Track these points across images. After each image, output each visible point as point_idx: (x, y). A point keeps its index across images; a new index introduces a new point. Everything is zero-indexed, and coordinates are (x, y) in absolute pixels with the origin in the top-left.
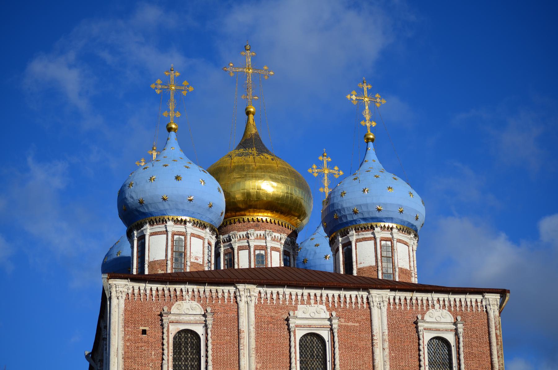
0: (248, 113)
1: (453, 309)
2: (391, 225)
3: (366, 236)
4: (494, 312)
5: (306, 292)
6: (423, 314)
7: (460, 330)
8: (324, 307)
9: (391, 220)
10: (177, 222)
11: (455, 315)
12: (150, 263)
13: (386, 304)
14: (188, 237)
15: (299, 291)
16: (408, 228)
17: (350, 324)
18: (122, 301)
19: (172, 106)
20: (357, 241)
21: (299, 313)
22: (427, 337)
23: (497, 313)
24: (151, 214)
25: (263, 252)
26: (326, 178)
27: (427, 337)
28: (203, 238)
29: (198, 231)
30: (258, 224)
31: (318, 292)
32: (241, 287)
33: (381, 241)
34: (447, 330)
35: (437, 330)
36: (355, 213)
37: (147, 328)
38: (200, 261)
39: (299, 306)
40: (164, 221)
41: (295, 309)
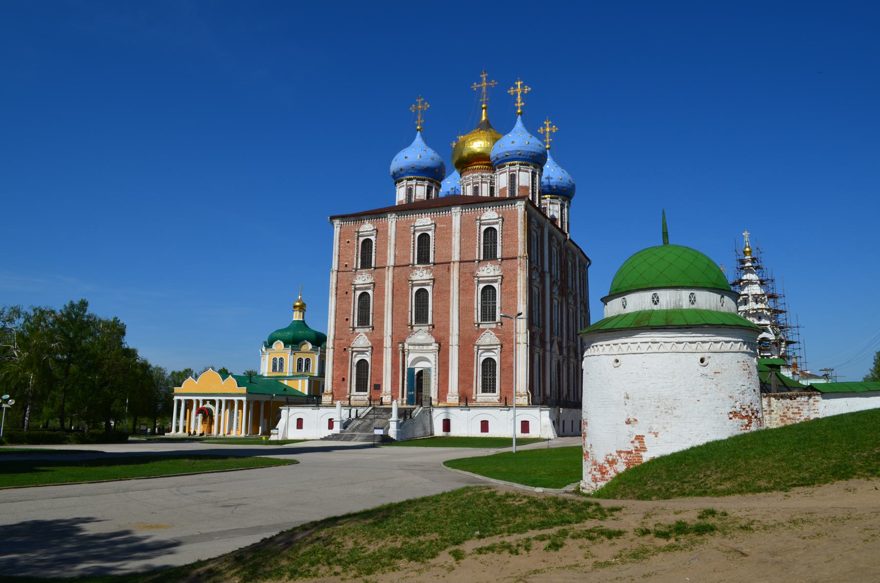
1: (498, 210)
2: (514, 162)
3: (503, 171)
6: (481, 216)
8: (429, 219)
10: (408, 180)
11: (499, 213)
13: (460, 213)
14: (414, 186)
17: (442, 226)
18: (339, 228)
19: (419, 117)
20: (500, 174)
23: (523, 210)
25: (477, 185)
26: (548, 134)
28: (424, 186)
29: (419, 182)
30: (474, 171)
33: (509, 172)
34: (494, 224)
35: (489, 224)
37: (349, 240)
38: (422, 198)
39: (417, 220)
41: (416, 221)
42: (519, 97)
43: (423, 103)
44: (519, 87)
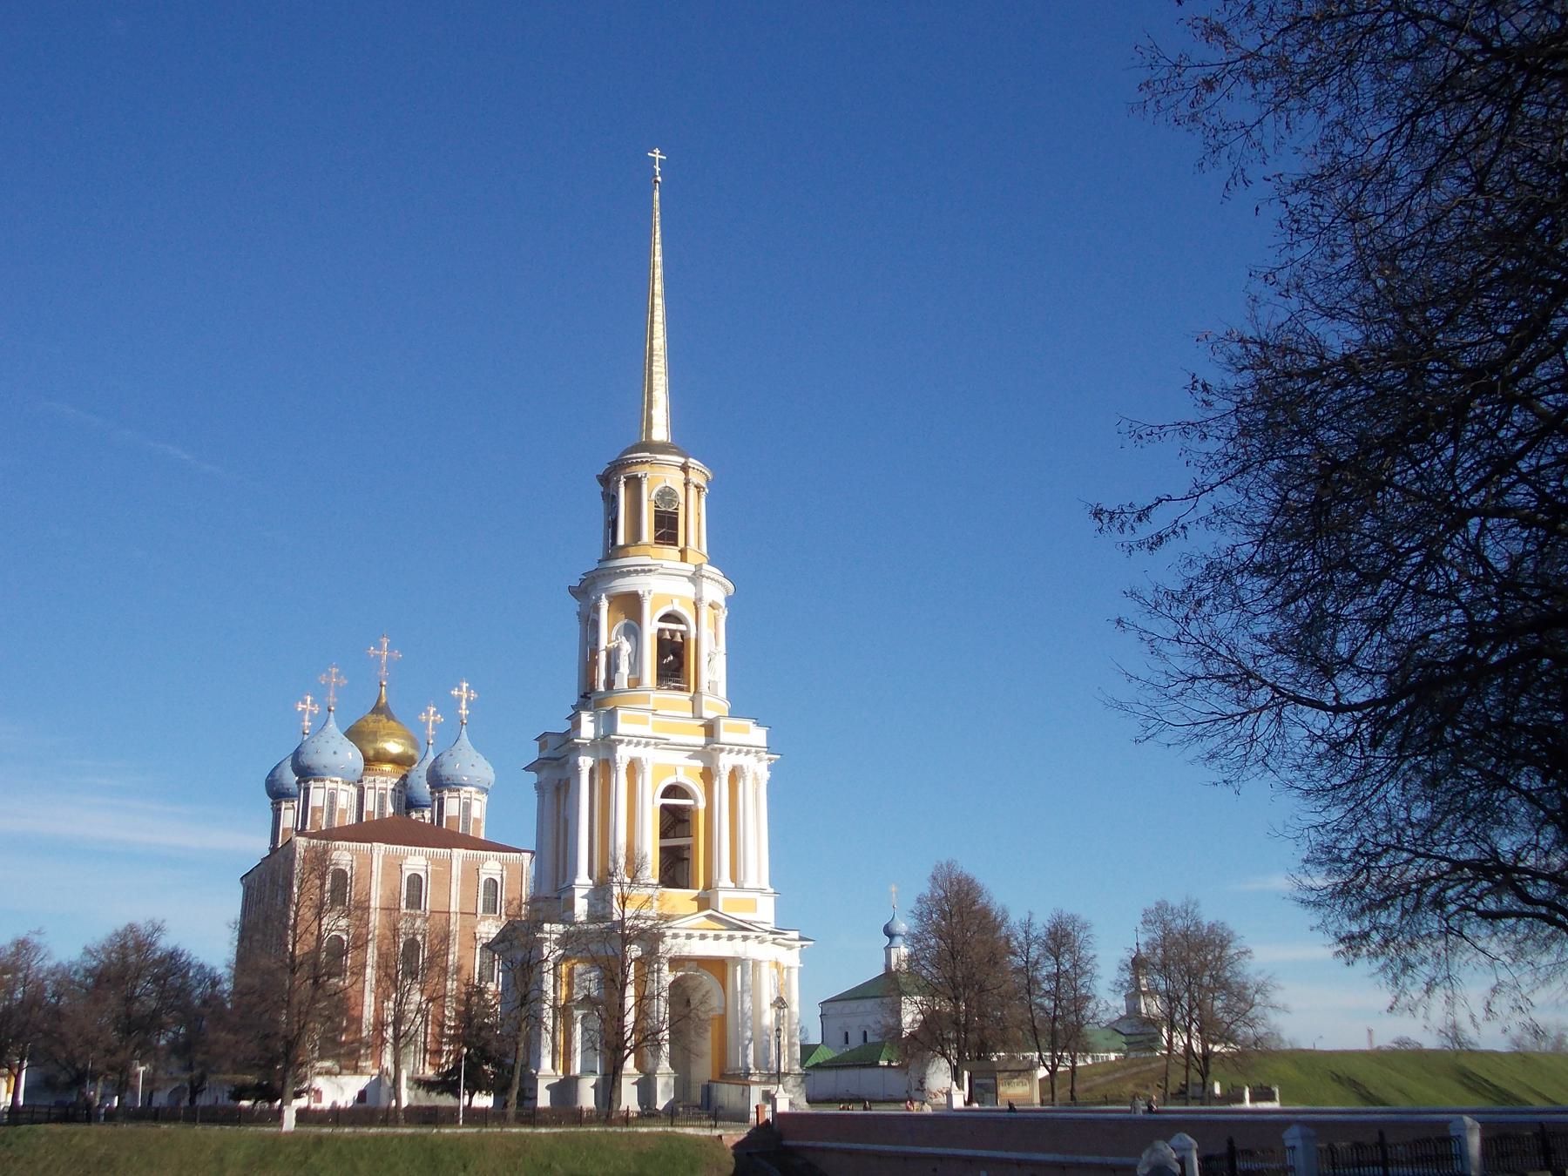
0: (381, 686)
4: (526, 863)
5: (414, 848)
7: (504, 875)
9: (472, 785)
10: (332, 781)
12: (313, 808)
15: (410, 848)
16: (484, 790)
21: (408, 861)
22: (483, 878)
24: (315, 774)
27: (483, 878)
29: (345, 787)
30: (382, 773)
31: (421, 849)
32: (374, 844)
36: (448, 779)
40: (323, 780)
42: (464, 702)
43: (337, 675)
44: (464, 689)
